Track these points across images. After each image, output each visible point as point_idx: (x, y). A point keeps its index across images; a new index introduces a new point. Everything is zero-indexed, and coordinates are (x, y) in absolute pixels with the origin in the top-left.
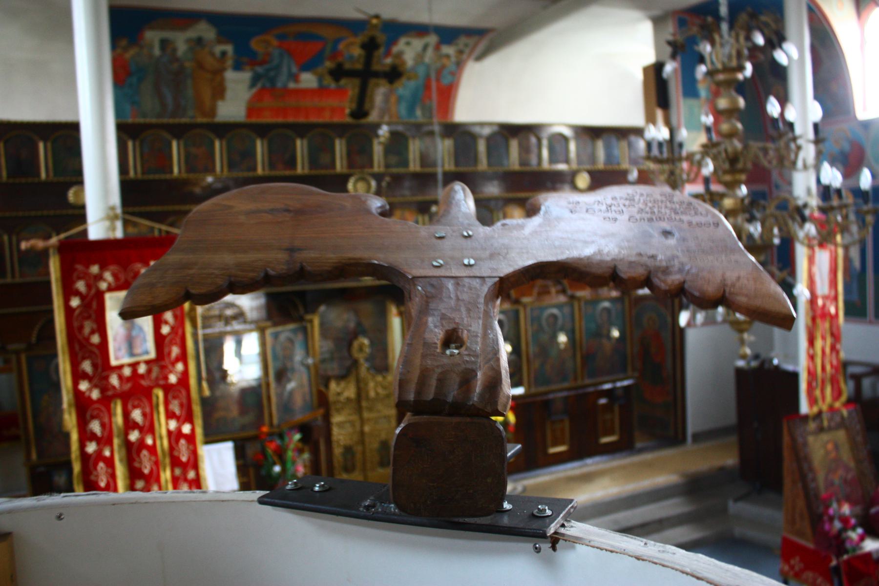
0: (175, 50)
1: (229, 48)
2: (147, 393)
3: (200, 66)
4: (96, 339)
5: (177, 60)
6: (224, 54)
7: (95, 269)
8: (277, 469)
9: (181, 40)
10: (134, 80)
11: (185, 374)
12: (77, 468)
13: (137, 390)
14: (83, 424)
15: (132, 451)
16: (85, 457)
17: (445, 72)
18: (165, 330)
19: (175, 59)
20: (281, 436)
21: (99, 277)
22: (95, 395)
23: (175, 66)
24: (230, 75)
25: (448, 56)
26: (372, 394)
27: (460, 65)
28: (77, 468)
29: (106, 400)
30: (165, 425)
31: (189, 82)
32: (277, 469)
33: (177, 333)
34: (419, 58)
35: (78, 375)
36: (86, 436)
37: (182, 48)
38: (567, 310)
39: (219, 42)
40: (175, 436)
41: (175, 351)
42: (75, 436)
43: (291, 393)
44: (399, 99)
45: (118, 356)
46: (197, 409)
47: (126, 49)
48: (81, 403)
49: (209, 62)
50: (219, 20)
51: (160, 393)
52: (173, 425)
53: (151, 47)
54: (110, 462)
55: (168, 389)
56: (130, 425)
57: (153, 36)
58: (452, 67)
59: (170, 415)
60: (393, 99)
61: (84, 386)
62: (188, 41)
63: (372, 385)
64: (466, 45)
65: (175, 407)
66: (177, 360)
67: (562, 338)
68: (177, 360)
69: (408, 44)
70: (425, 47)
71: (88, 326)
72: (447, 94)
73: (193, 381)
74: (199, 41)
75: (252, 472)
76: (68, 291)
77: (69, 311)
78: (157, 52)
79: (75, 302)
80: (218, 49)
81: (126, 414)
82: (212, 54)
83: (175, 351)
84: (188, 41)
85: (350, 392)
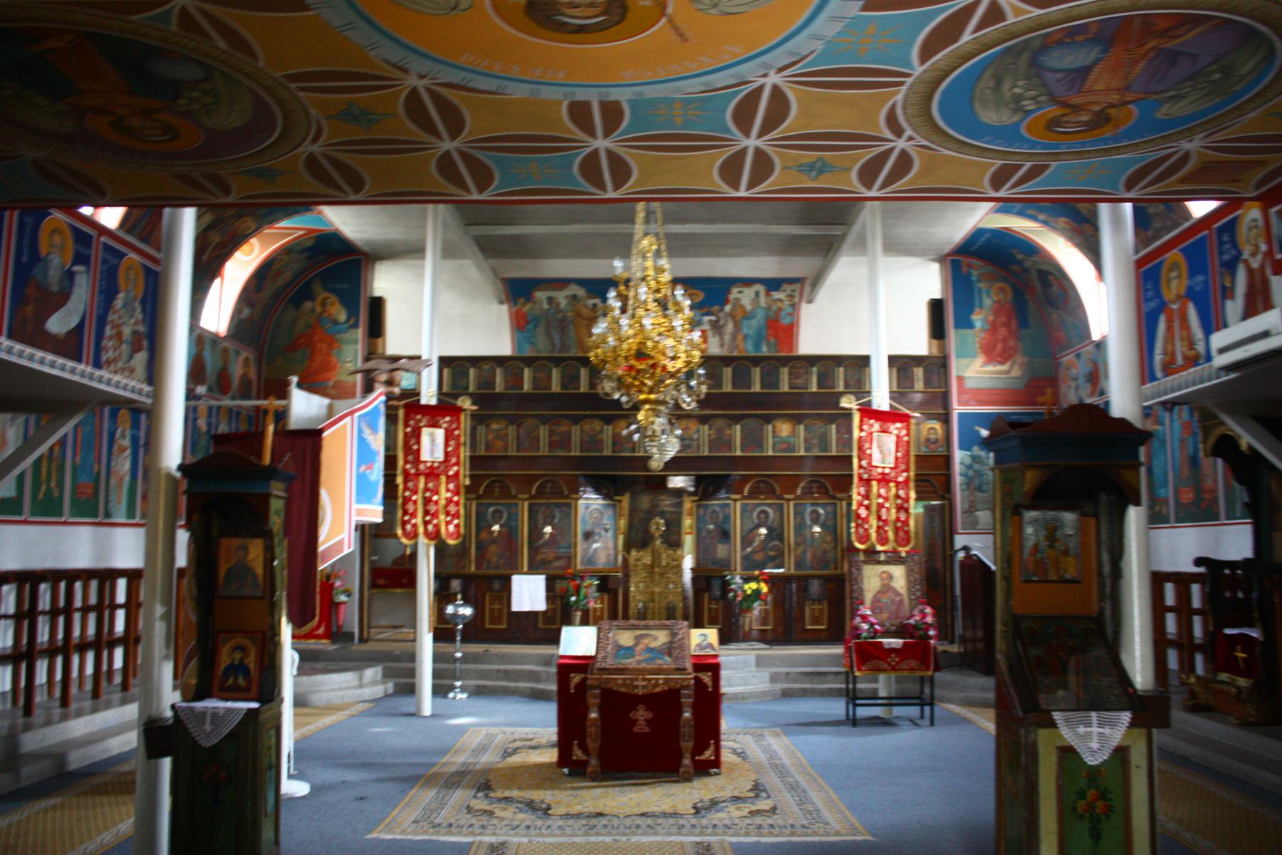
0: (558, 304)
2: (437, 476)
3: (579, 315)
4: (415, 447)
5: (561, 311)
6: (595, 305)
7: (419, 417)
8: (573, 599)
9: (562, 297)
10: (530, 326)
12: (400, 501)
13: (432, 473)
14: (406, 482)
15: (427, 501)
16: (404, 498)
17: (783, 313)
18: (450, 449)
20: (582, 578)
21: (420, 421)
22: (413, 471)
23: (560, 315)
26: (664, 563)
27: (795, 307)
28: (400, 501)
29: (418, 475)
30: (444, 495)
31: (571, 327)
32: (573, 599)
35: (406, 462)
36: (406, 489)
37: (563, 303)
38: (830, 509)
40: (449, 501)
41: (454, 460)
42: (401, 487)
43: (596, 550)
44: (746, 337)
45: (425, 456)
46: (462, 490)
48: (406, 474)
50: (582, 282)
51: (443, 479)
52: (449, 495)
54: (415, 502)
55: (448, 477)
56: (426, 489)
57: (541, 295)
58: (790, 310)
59: (448, 490)
60: (740, 337)
61: (408, 466)
63: (664, 555)
65: (451, 486)
67: (817, 529)
70: (757, 294)
71: (413, 441)
73: (461, 477)
74: (574, 297)
75: (558, 601)
76: (406, 425)
77: (406, 434)
78: (546, 306)
79: (409, 430)
80: (591, 302)
81: (426, 484)
82: (586, 306)
83: (454, 460)
85: (647, 560)
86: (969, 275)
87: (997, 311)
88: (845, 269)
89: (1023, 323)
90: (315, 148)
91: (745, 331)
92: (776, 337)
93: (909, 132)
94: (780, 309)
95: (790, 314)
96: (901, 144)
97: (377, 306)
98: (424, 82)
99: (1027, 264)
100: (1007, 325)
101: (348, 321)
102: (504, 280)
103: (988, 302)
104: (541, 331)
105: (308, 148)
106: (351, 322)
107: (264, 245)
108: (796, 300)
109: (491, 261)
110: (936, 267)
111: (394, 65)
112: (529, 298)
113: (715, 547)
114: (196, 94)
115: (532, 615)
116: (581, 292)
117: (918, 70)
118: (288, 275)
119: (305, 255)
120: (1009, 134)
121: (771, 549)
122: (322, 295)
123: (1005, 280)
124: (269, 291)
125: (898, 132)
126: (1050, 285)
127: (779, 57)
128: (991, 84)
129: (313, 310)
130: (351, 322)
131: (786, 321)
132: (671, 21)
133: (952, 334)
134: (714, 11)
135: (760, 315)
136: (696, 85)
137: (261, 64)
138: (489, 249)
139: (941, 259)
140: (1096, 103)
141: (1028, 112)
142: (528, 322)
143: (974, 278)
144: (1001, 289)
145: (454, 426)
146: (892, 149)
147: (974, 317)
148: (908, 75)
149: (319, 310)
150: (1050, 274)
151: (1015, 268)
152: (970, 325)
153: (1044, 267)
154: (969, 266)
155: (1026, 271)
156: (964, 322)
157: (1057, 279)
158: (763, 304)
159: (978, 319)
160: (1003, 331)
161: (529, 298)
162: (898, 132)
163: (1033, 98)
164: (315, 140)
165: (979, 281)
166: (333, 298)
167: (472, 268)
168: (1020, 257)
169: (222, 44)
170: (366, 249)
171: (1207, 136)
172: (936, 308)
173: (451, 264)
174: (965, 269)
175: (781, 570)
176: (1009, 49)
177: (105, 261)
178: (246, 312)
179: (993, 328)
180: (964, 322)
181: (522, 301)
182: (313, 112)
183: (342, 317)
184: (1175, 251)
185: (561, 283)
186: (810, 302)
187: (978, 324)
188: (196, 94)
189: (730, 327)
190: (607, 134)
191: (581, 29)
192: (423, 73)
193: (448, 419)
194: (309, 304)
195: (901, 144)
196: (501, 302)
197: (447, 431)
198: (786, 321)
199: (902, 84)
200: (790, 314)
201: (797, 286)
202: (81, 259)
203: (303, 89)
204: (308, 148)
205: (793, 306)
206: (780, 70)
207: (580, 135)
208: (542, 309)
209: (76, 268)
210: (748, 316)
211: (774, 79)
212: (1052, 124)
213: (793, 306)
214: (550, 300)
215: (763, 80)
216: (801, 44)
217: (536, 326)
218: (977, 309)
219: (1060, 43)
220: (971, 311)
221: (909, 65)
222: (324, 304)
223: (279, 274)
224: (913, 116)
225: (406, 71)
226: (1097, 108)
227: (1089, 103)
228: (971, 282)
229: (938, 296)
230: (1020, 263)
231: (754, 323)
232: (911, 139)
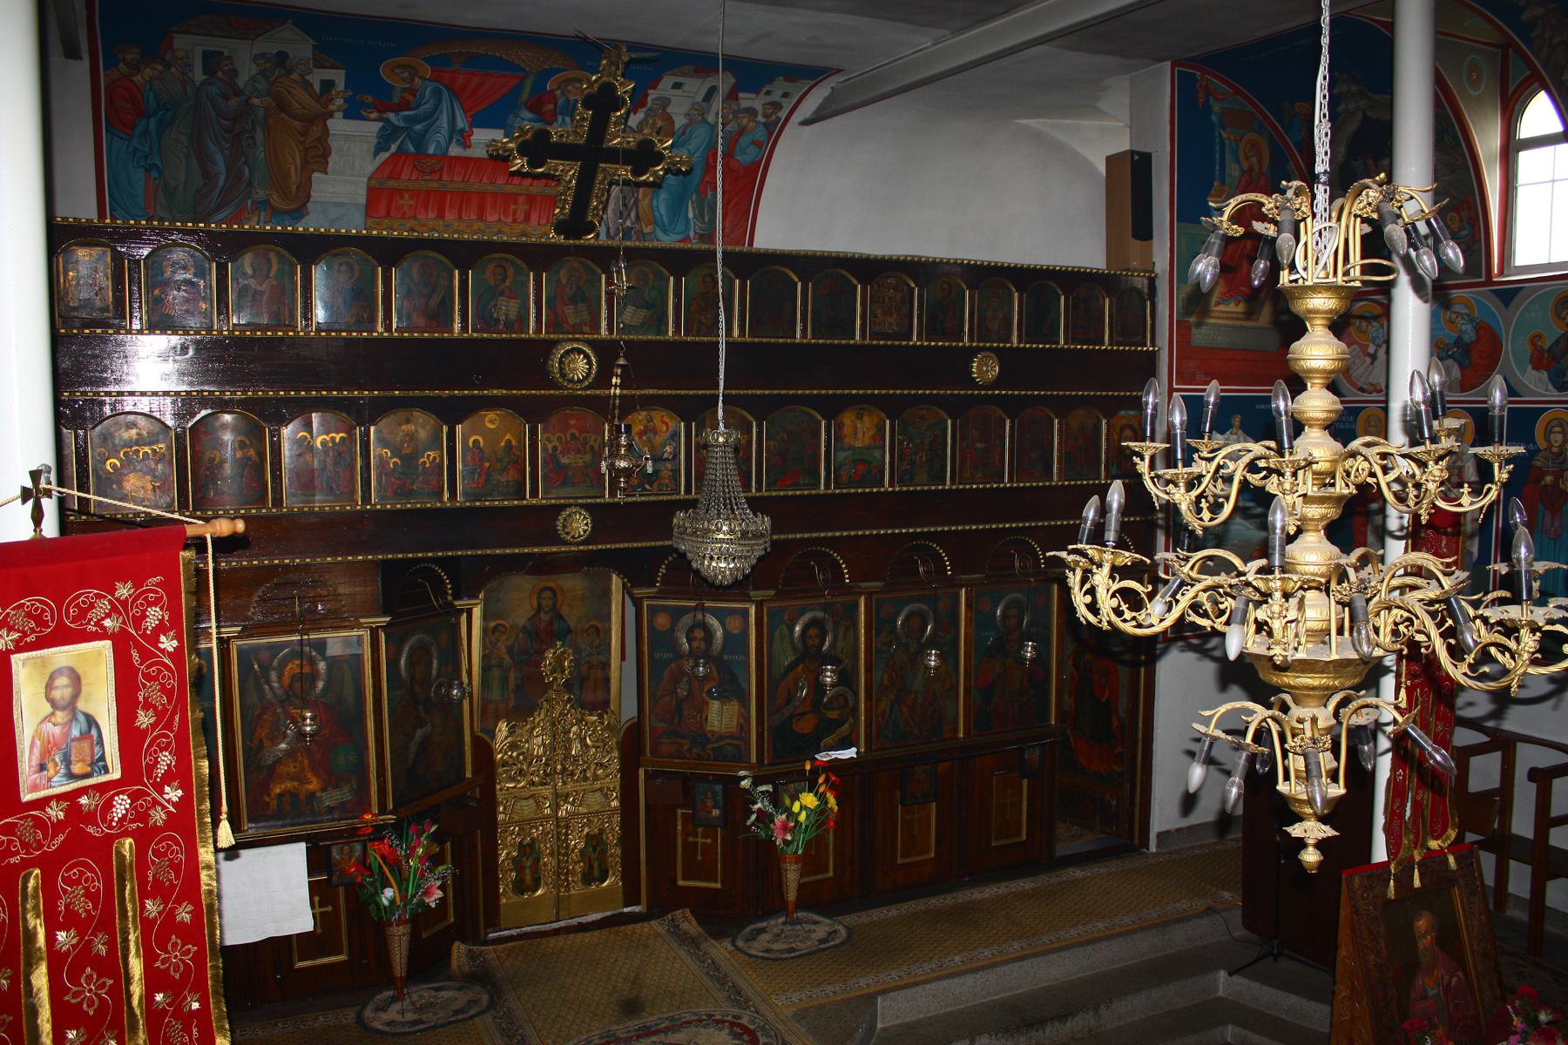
0: (234, 73)
1: (339, 77)
3: (282, 106)
5: (238, 92)
6: (328, 85)
11: (185, 804)
23: (234, 102)
24: (338, 125)
25: (751, 112)
31: (260, 135)
33: (169, 726)
34: (698, 114)
39: (320, 65)
41: (166, 759)
58: (760, 134)
64: (785, 95)
66: (168, 778)
68: (168, 778)
69: (677, 86)
72: (745, 187)
78: (198, 75)
80: (317, 77)
82: (308, 86)
95: (758, 144)
108: (783, 114)
113: (702, 707)
115: (277, 948)
116: (302, 49)
121: (828, 707)
145: (154, 615)
165: (1222, 126)
175: (850, 753)
193: (124, 591)
197: (122, 644)
200: (758, 144)
214: (212, 61)
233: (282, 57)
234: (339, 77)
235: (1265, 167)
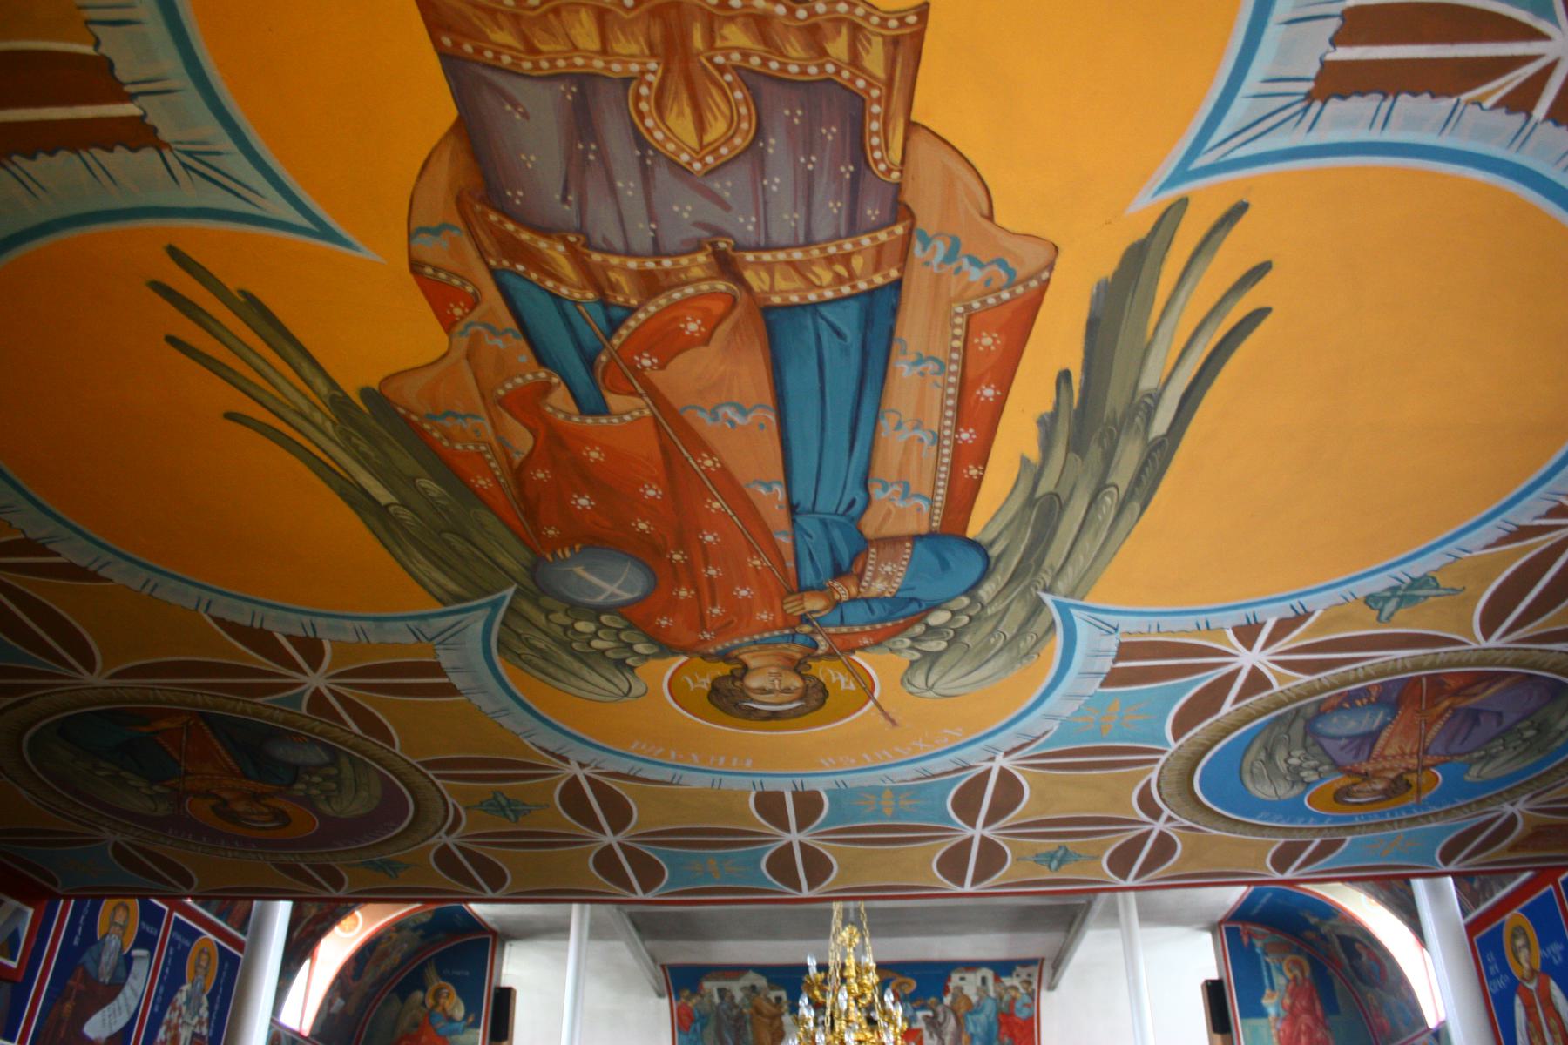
0: (733, 998)
3: (758, 1011)
5: (736, 1006)
6: (779, 999)
9: (737, 988)
19: (734, 1006)
23: (735, 1012)
25: (1014, 988)
31: (749, 1027)
37: (739, 996)
39: (772, 989)
47: (688, 999)
49: (766, 1007)
53: (712, 996)
57: (711, 987)
58: (1027, 999)
62: (743, 989)
69: (962, 979)
70: (984, 980)
78: (717, 1000)
80: (773, 995)
82: (769, 1000)
84: (743, 989)
86: (1252, 946)
87: (1294, 994)
88: (1094, 947)
89: (1331, 1006)
90: (451, 841)
91: (971, 1028)
92: (1012, 1036)
93: (1167, 812)
94: (1014, 999)
95: (1025, 1005)
96: (1159, 826)
97: (505, 998)
98: (587, 771)
99: (1325, 929)
100: (1310, 1010)
101: (466, 1017)
102: (663, 967)
103: (1280, 981)
104: (710, 1032)
105: (441, 839)
106: (471, 1020)
107: (369, 919)
108: (1035, 986)
109: (649, 944)
110: (1207, 937)
111: (552, 754)
112: (695, 989)
114: (316, 779)
116: (761, 982)
117: (1173, 746)
118: (396, 957)
119: (420, 932)
120: (1292, 809)
122: (435, 982)
123: (1299, 952)
124: (369, 977)
125: (1155, 813)
126: (1359, 956)
127: (1008, 739)
128: (1263, 756)
129: (424, 1004)
130: (471, 1020)
131: (1022, 1014)
132: (877, 704)
133: (1239, 1024)
134: (930, 694)
135: (990, 1007)
136: (907, 773)
137: (397, 750)
138: (647, 927)
139: (1214, 928)
140: (1392, 769)
141: (1309, 784)
142: (693, 1021)
143: (1258, 951)
144: (1295, 963)
146: (1148, 833)
147: (1265, 1002)
148: (1162, 752)
149: (430, 1002)
150: (1357, 940)
151: (1309, 934)
152: (1261, 1013)
153: (1347, 933)
154: (1250, 935)
155: (1324, 938)
156: (1253, 1010)
157: (1366, 947)
158: (992, 994)
159: (1270, 1004)
160: (1305, 1019)
161: (695, 989)
162: (1155, 813)
163: (1315, 769)
164: (448, 833)
166: (450, 988)
167: (624, 952)
168: (1313, 920)
169: (355, 728)
170: (494, 926)
171: (1533, 797)
172: (1214, 991)
173: (600, 946)
174: (1245, 939)
176: (1279, 717)
177: (173, 943)
178: (339, 1002)
179: (1292, 1015)
180: (1253, 1010)
181: (687, 993)
182: (450, 800)
183: (460, 1012)
184: (1515, 911)
185: (736, 971)
186: (1051, 988)
187: (1272, 1011)
188: (316, 779)
189: (951, 1024)
190: (800, 828)
191: (774, 715)
192: (584, 761)
194: (419, 995)
195: (1159, 826)
196: (660, 995)
198: (1022, 1014)
199: (1156, 761)
200: (1029, 1006)
201: (1034, 970)
202: (145, 940)
203: (438, 776)
204: (441, 839)
205: (1031, 995)
206: (1007, 754)
207: (770, 828)
208: (711, 1003)
209: (136, 952)
210: (973, 1009)
211: (1001, 762)
212: (1340, 796)
213: (1031, 995)
214: (722, 992)
215: (988, 765)
216: (1033, 725)
217: (703, 1026)
218: (1268, 991)
219: (1338, 708)
220: (1261, 994)
221: (1164, 741)
222: (437, 995)
223: (385, 954)
224: (1170, 796)
225: (566, 760)
226: (1392, 775)
227: (1384, 769)
228: (1256, 956)
229: (1214, 976)
230: (1315, 928)
231: (982, 1018)
232: (1170, 819)
233: (753, 987)
234: (783, 994)
235: (1307, 974)
